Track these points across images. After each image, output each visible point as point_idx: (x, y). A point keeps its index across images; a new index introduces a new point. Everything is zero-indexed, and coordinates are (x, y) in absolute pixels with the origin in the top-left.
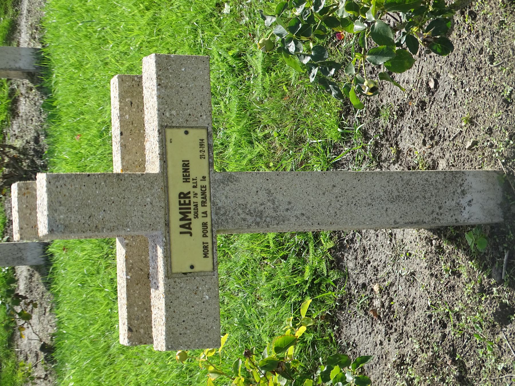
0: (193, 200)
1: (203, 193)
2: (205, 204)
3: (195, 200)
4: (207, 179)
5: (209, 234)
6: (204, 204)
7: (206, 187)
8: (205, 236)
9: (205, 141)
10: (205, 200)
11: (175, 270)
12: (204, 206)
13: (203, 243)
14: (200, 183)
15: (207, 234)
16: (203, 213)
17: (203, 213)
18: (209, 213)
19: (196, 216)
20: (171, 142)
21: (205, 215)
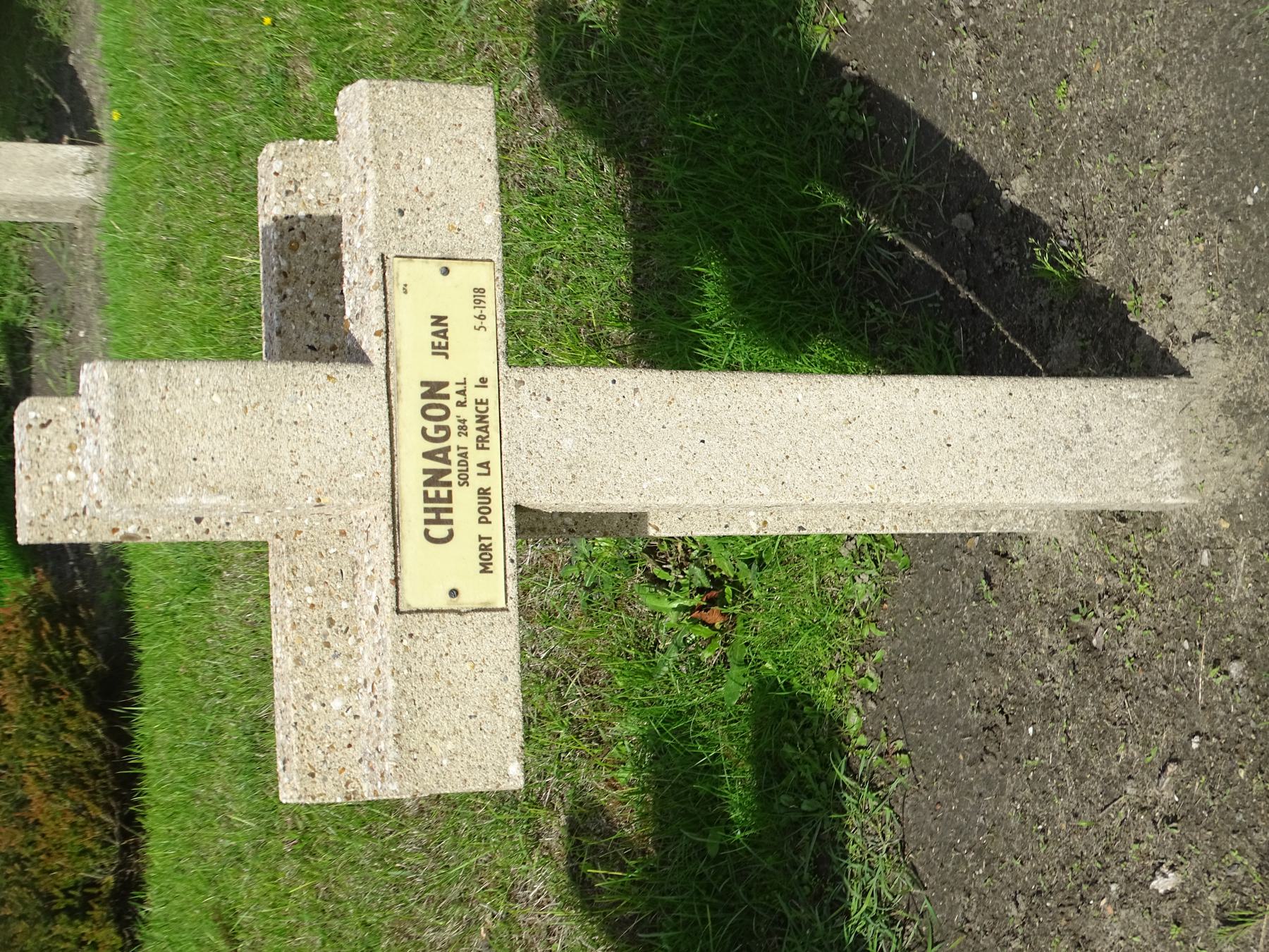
1: (482, 418)
2: (486, 445)
4: (492, 382)
6: (482, 443)
7: (487, 403)
8: (483, 520)
10: (484, 435)
12: (483, 448)
13: (480, 538)
14: (473, 394)
16: (480, 465)
17: (480, 465)
20: (406, 292)
21: (486, 471)
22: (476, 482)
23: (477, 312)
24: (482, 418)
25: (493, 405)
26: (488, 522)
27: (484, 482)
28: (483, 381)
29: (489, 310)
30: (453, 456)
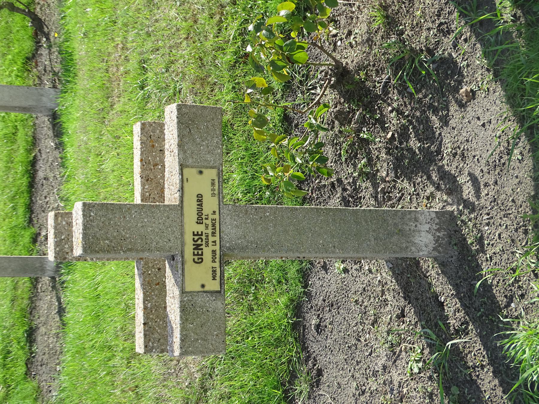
1: (214, 225)
3: (207, 231)
4: (217, 213)
5: (217, 260)
6: (213, 234)
8: (213, 261)
9: (216, 181)
11: (187, 290)
12: (214, 236)
13: (213, 268)
14: (211, 217)
15: (216, 260)
16: (213, 242)
17: (213, 242)
19: (207, 245)
20: (187, 181)
22: (211, 248)
23: (212, 188)
24: (214, 225)
26: (215, 262)
27: (214, 248)
30: (204, 237)
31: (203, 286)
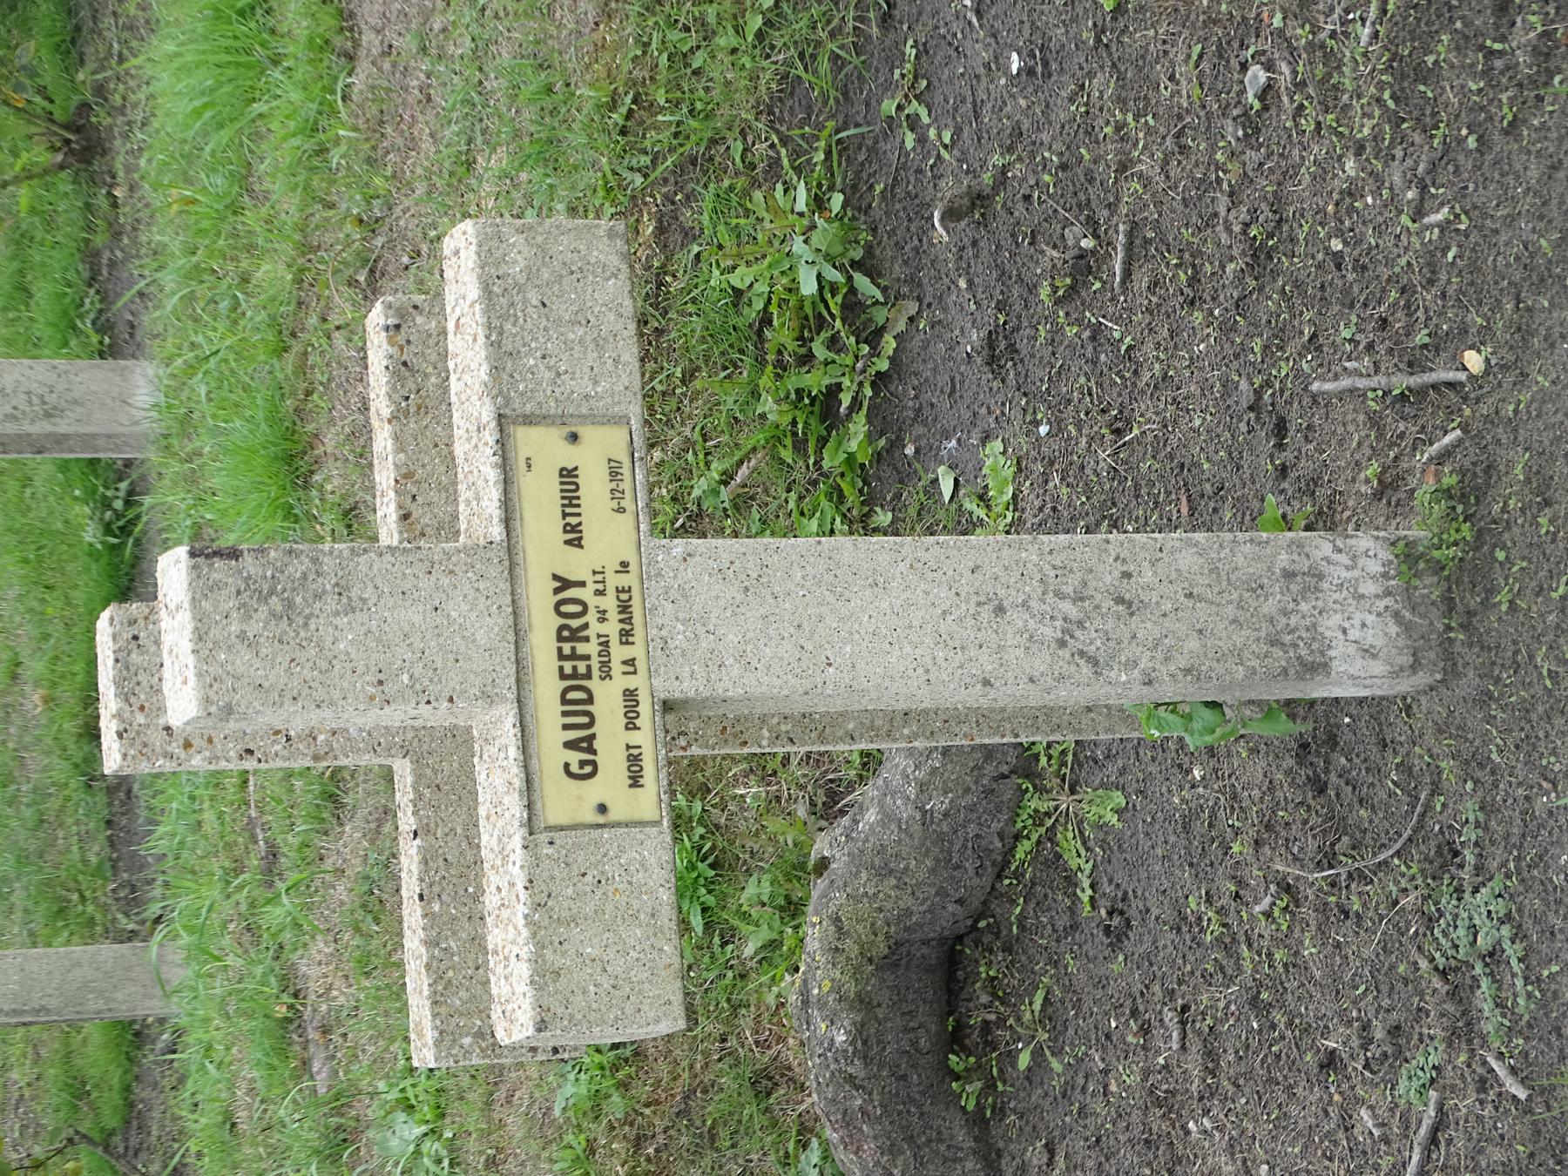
0: (595, 628)
1: (624, 608)
6: (626, 636)
8: (631, 726)
12: (627, 643)
13: (628, 747)
14: (613, 581)
15: (637, 722)
16: (625, 663)
17: (625, 663)
18: (641, 664)
19: (607, 675)
22: (620, 682)
23: (614, 485)
24: (624, 608)
25: (636, 594)
26: (636, 728)
27: (631, 682)
28: (625, 564)
29: (626, 485)
31: (602, 809)
